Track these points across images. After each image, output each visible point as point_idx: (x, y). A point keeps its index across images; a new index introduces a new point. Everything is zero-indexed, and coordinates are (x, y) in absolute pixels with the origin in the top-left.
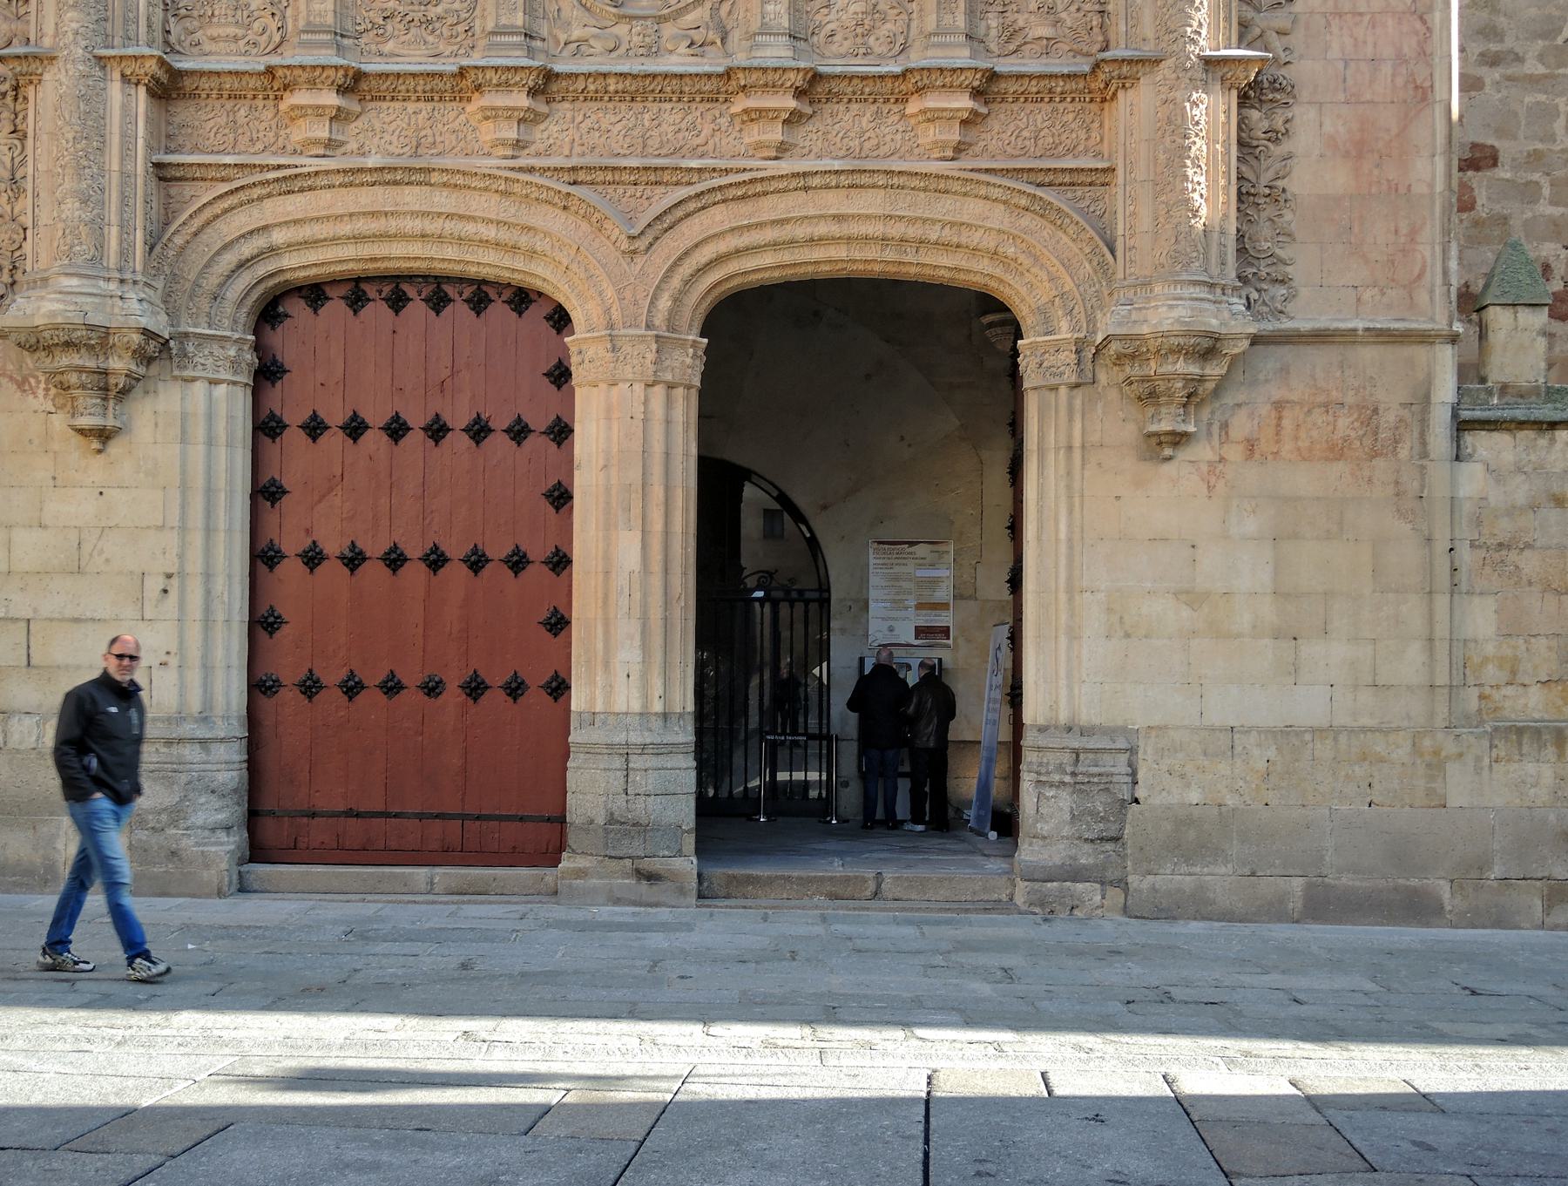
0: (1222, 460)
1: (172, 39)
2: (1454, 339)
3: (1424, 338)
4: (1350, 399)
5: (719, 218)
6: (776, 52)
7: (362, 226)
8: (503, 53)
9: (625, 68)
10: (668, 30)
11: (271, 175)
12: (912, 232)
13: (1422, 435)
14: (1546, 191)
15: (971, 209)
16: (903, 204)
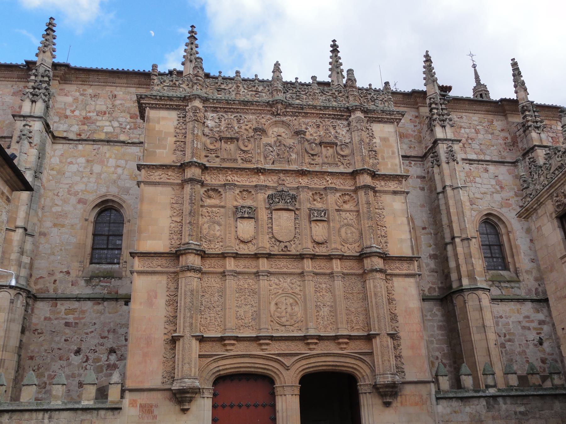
0: (397, 406)
1: (201, 330)
2: (433, 382)
3: (428, 382)
4: (417, 394)
5: (304, 362)
6: (312, 332)
7: (236, 366)
9: (285, 335)
10: (292, 328)
11: (221, 356)
12: (338, 364)
13: (430, 400)
14: (435, 342)
15: (348, 360)
16: (336, 359)
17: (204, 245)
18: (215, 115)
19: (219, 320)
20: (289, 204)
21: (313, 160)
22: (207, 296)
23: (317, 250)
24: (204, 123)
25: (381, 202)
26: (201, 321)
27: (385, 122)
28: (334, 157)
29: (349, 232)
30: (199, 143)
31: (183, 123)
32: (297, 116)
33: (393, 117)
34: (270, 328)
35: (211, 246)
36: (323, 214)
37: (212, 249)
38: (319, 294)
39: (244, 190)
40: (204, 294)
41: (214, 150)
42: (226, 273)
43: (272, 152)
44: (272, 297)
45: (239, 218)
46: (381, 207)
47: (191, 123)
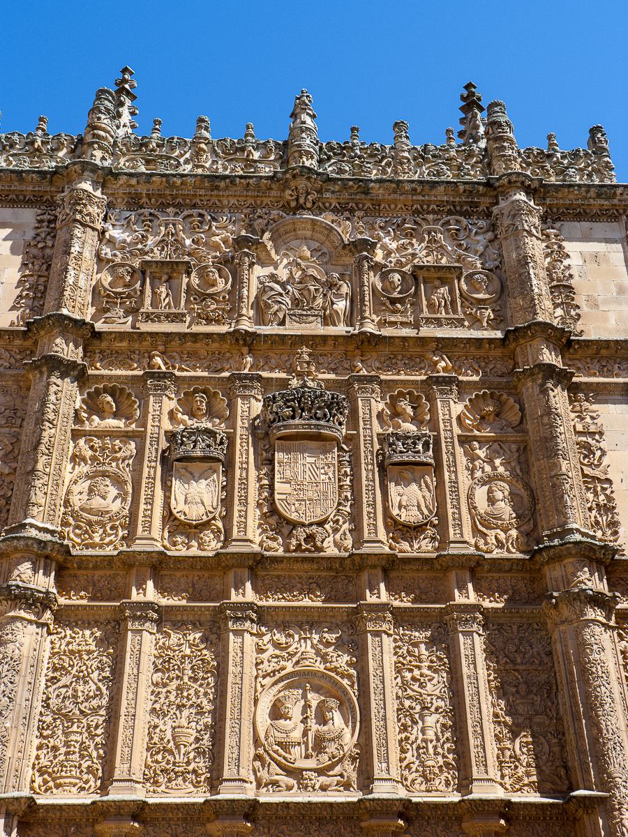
1: (36, 785)
8: (231, 791)
10: (323, 779)
17: (72, 536)
18: (133, 213)
19: (95, 754)
20: (322, 423)
21: (395, 312)
22: (65, 680)
23: (405, 545)
24: (104, 232)
25: (594, 415)
26: (38, 758)
27: (595, 218)
28: (453, 302)
29: (499, 495)
30: (82, 276)
31: (49, 234)
32: (352, 211)
33: (616, 201)
34: (252, 778)
35: (91, 538)
36: (420, 447)
37: (93, 546)
38: (408, 675)
39: (196, 391)
40: (57, 674)
41: (124, 293)
42: (128, 613)
43: (281, 295)
44: (265, 682)
45: (178, 460)
46: (592, 429)
47: (64, 229)
